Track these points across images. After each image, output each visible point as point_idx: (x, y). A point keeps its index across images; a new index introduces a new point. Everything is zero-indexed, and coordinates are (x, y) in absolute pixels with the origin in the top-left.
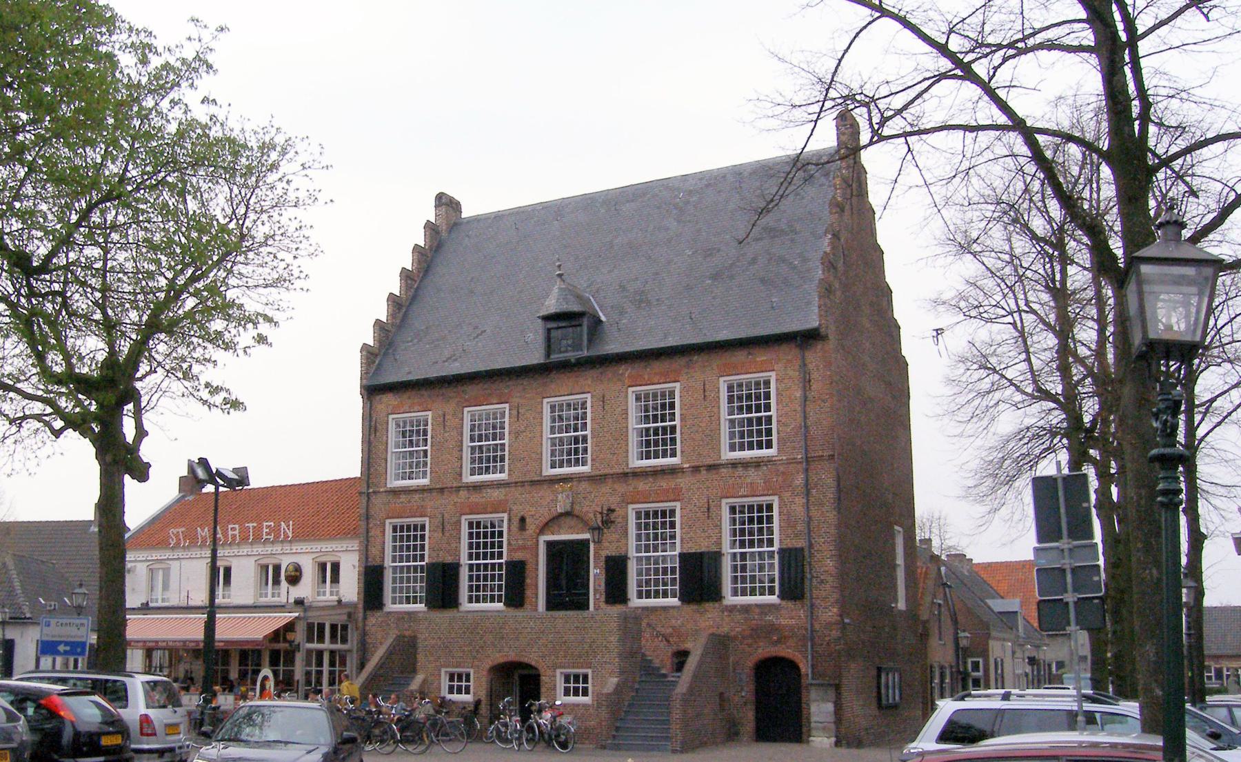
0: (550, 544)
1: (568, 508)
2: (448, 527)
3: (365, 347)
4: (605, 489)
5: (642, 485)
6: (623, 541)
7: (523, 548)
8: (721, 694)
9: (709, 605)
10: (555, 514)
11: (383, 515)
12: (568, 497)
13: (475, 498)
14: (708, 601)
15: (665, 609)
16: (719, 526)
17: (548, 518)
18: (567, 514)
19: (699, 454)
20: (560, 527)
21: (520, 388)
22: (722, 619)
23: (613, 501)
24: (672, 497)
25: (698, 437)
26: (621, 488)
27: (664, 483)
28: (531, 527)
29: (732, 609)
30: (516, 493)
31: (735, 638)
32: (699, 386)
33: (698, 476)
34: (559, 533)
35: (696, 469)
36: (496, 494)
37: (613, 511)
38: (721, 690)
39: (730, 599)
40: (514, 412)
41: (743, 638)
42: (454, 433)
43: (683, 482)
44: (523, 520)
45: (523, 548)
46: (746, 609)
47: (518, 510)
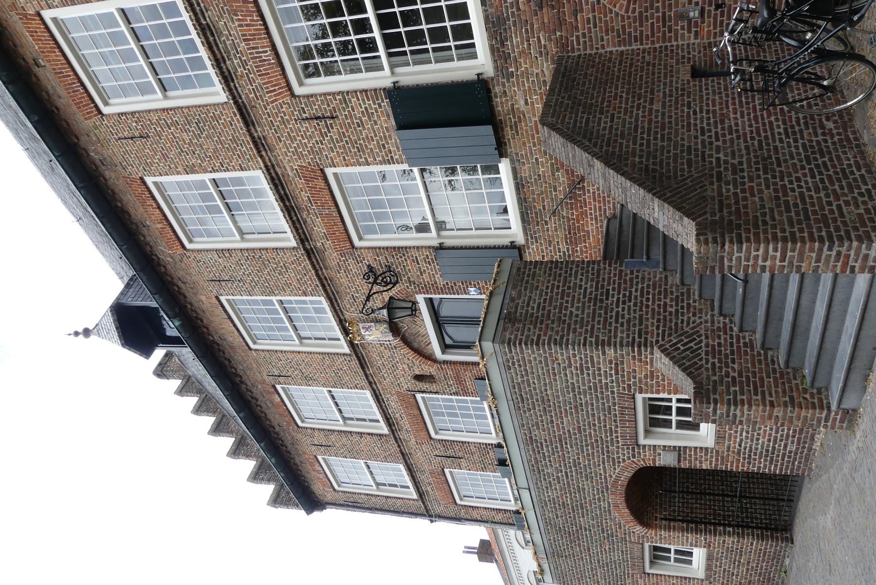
0: (445, 347)
1: (384, 327)
2: (450, 452)
3: (277, 500)
4: (341, 280)
5: (318, 228)
6: (415, 253)
7: (459, 380)
8: (696, 73)
9: (501, 105)
10: (397, 342)
11: (452, 507)
12: (367, 329)
13: (405, 423)
14: (492, 109)
15: (519, 186)
16: (345, 95)
17: (406, 350)
18: (394, 329)
19: (234, 140)
20: (417, 335)
21: (248, 372)
22: (527, 74)
23: (356, 269)
24: (321, 184)
25: (209, 145)
26: (332, 257)
27: (302, 195)
28: (428, 369)
29: (498, 52)
30: (385, 383)
31: (563, 44)
32: (130, 146)
33: (271, 139)
34: (426, 335)
35: (259, 144)
36: (394, 405)
37: (371, 269)
38: (685, 73)
39: (482, 62)
40: (281, 379)
41: (560, 23)
42: (333, 437)
43: (289, 166)
44: (419, 378)
45: (459, 380)
46: (496, 26)
47: (407, 383)
